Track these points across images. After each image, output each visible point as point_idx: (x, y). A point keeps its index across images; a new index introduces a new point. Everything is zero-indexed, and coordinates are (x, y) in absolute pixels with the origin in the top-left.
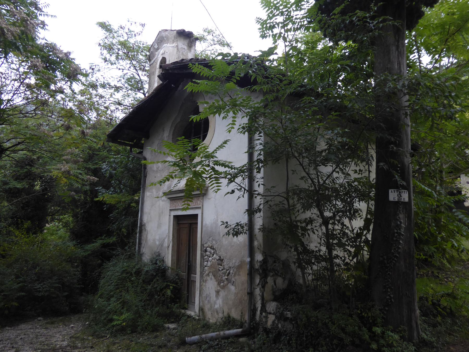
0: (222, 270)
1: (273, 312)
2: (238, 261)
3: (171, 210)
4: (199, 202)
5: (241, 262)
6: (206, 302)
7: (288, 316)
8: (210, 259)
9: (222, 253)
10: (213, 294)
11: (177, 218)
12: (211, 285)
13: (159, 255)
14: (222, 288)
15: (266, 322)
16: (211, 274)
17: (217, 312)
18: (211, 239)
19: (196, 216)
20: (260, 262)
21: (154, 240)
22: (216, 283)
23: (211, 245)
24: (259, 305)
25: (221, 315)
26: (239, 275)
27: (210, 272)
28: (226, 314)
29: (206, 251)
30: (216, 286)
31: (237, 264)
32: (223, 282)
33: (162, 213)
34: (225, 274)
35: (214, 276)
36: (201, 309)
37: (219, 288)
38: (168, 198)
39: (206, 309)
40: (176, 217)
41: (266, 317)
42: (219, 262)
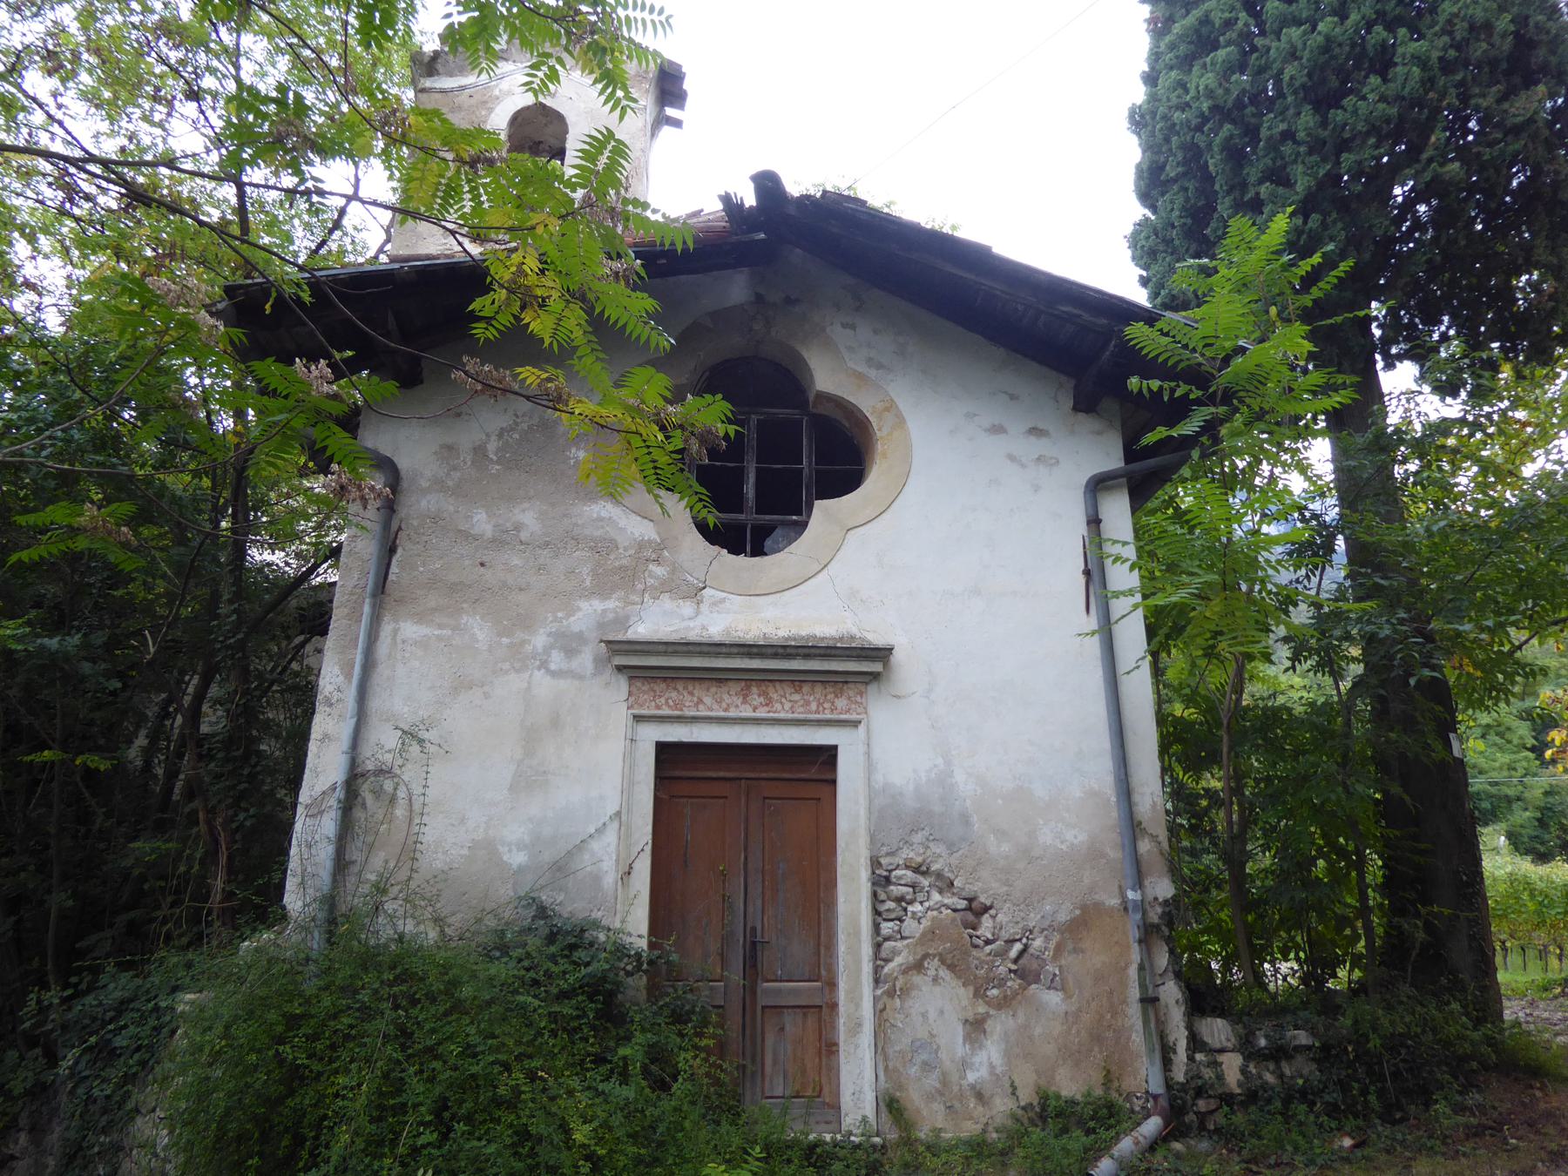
0: (988, 942)
1: (1230, 1045)
2: (1068, 905)
3: (638, 719)
4: (841, 703)
5: (1084, 908)
6: (913, 1071)
7: (1297, 1043)
8: (917, 908)
9: (985, 887)
10: (952, 1039)
11: (666, 753)
12: (938, 1005)
13: (542, 912)
14: (999, 1007)
15: (1220, 1077)
16: (932, 966)
17: (980, 1096)
18: (918, 838)
19: (826, 757)
20: (1166, 902)
21: (487, 848)
22: (965, 994)
23: (919, 859)
24: (1179, 1036)
25: (1002, 1106)
26: (1075, 951)
27: (926, 956)
28: (1027, 1095)
29: (888, 880)
30: (965, 1002)
31: (1063, 917)
32: (1002, 983)
33: (555, 723)
34: (1002, 954)
35: (951, 967)
36: (892, 1105)
37: (982, 1009)
38: (620, 669)
39: (914, 1098)
40: (663, 749)
41: (1215, 1064)
42: (970, 917)
